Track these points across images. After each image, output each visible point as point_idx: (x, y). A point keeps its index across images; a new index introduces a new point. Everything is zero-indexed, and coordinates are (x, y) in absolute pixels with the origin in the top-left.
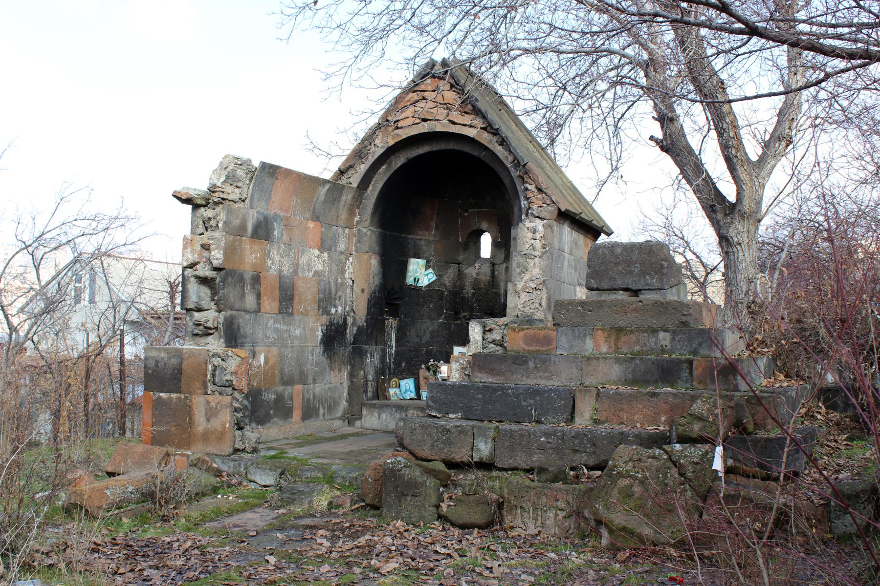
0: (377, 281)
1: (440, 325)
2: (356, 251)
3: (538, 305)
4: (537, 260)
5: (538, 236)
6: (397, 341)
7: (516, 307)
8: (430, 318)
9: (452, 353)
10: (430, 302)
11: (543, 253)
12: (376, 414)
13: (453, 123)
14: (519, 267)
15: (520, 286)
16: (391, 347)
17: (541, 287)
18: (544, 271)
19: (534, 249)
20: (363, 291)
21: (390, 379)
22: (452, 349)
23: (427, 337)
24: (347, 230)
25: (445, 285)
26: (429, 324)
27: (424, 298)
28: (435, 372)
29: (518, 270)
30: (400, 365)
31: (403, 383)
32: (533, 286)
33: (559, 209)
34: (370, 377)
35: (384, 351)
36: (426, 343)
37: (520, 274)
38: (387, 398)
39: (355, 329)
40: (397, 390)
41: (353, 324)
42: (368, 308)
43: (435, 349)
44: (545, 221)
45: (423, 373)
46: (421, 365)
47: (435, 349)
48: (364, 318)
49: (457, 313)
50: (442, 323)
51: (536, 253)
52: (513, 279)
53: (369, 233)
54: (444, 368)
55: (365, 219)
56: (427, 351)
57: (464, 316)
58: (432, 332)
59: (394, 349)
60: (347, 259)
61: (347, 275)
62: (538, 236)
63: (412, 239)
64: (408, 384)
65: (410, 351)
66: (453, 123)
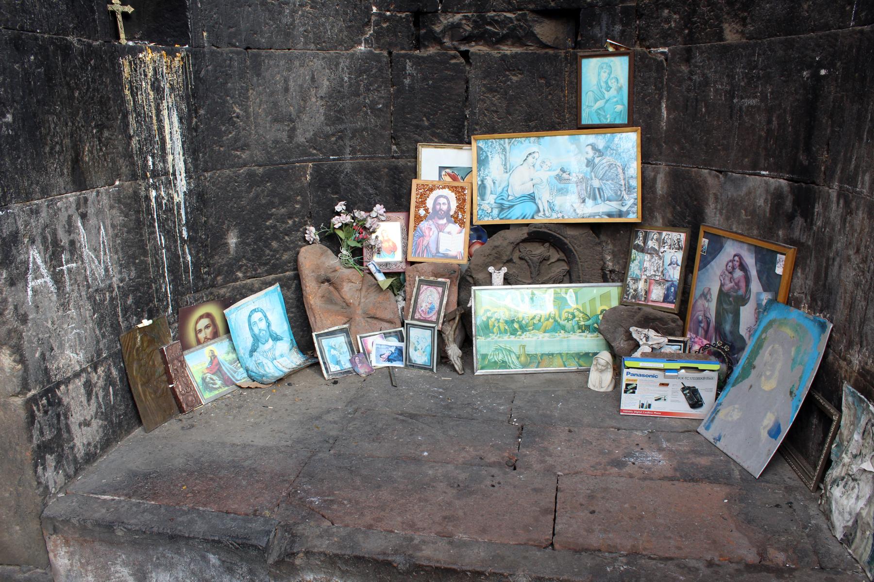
1: (361, 67)
6: (192, 148)
8: (320, 42)
9: (414, 172)
16: (166, 177)
21: (182, 314)
22: (414, 156)
23: (314, 119)
26: (317, 64)
28: (357, 252)
30: (218, 241)
31: (239, 314)
34: (71, 358)
35: (134, 207)
36: (313, 142)
38: (176, 403)
40: (220, 349)
43: (348, 163)
45: (313, 258)
46: (300, 227)
47: (348, 163)
49: (421, 17)
50: (369, 57)
54: (387, 232)
56: (317, 170)
57: (454, 28)
58: (335, 95)
59: (182, 184)
64: (262, 311)
65: (253, 180)
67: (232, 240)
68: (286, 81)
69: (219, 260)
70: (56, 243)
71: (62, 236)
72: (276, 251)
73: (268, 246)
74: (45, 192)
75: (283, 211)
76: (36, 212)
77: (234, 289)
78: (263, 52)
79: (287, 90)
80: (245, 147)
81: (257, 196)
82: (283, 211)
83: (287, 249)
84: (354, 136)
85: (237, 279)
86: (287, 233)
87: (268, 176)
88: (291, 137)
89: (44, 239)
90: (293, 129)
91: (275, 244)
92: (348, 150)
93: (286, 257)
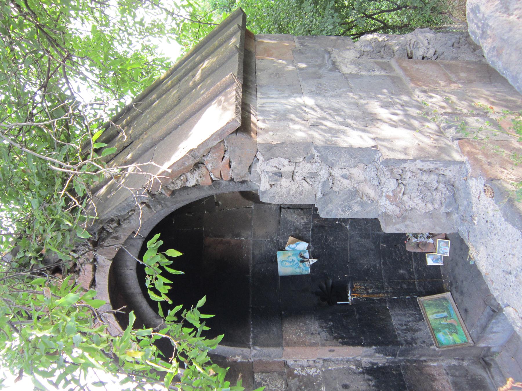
0: (314, 325)
2: (280, 358)
3: (433, 177)
4: (337, 172)
5: (287, 168)
7: (430, 215)
10: (327, 240)
11: (324, 160)
12: (491, 335)
13: (93, 283)
14: (349, 207)
15: (391, 208)
17: (397, 171)
18: (361, 161)
19: (314, 175)
20: (331, 351)
24: (257, 377)
25: (306, 224)
27: (323, 248)
29: (357, 208)
32: (392, 184)
33: (237, 131)
36: (374, 243)
37: (362, 204)
39: (377, 355)
41: (370, 356)
42: (354, 344)
44: (259, 156)
48: (365, 349)
51: (323, 173)
52: (371, 216)
53: (257, 348)
55: (240, 352)
56: (383, 243)
60: (291, 374)
61: (312, 372)
62: (287, 168)
63: (253, 266)
65: (385, 264)
66: (93, 283)
67: (401, 271)
68: (357, 251)
69: (407, 277)
70: (405, 330)
71: (404, 327)
72: (405, 257)
73: (403, 260)
74: (394, 331)
75: (394, 254)
76: (399, 334)
77: (416, 272)
78: (349, 258)
79: (359, 251)
80: (376, 266)
81: (389, 262)
82: (394, 254)
83: (405, 254)
84: (374, 231)
85: (413, 271)
86: (400, 254)
87: (384, 259)
88: (372, 250)
89: (405, 333)
90: (371, 249)
91: (403, 258)
92: (378, 233)
93: (407, 254)
